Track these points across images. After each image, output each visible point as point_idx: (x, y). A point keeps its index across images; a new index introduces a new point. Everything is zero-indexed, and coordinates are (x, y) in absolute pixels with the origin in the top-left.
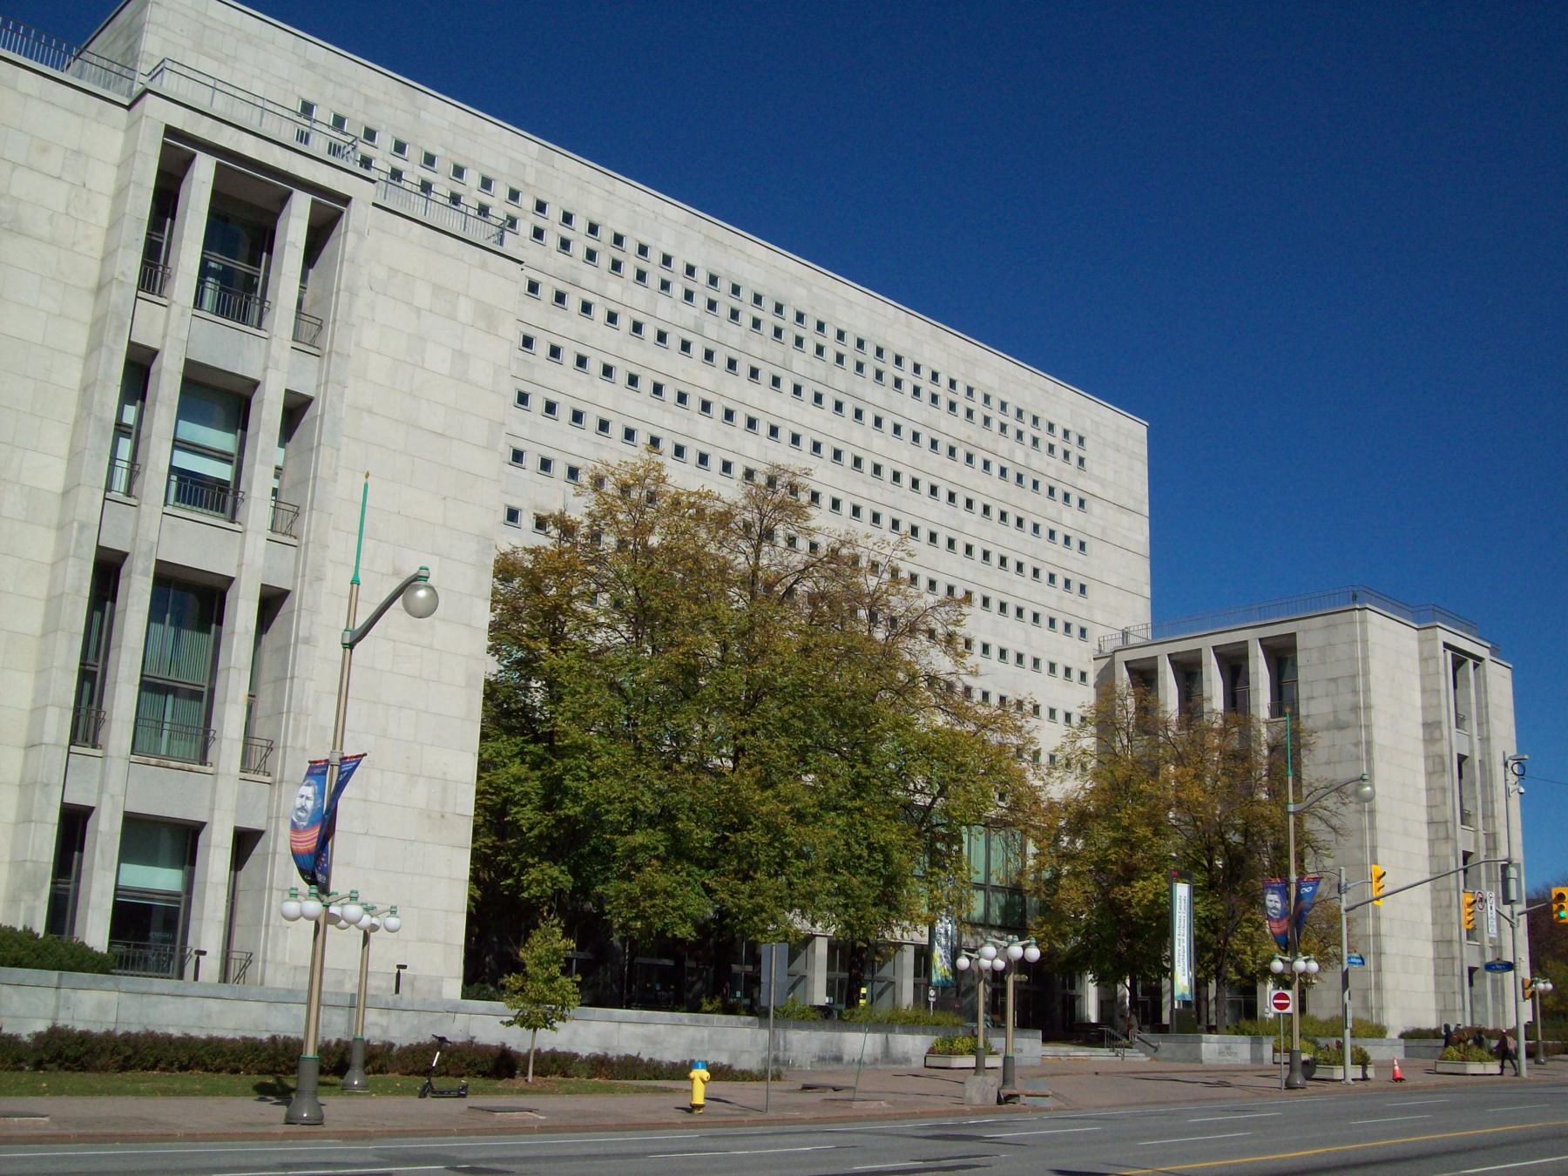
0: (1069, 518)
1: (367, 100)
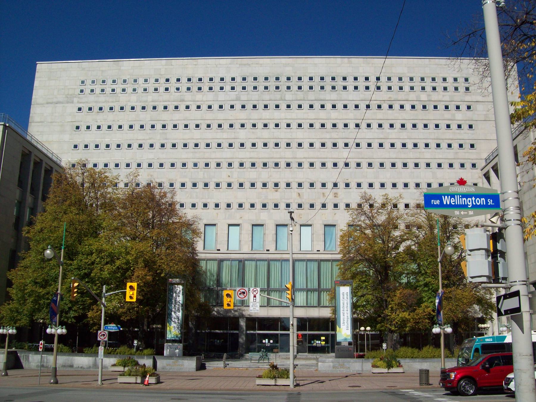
0: (461, 116)
1: (102, 71)
